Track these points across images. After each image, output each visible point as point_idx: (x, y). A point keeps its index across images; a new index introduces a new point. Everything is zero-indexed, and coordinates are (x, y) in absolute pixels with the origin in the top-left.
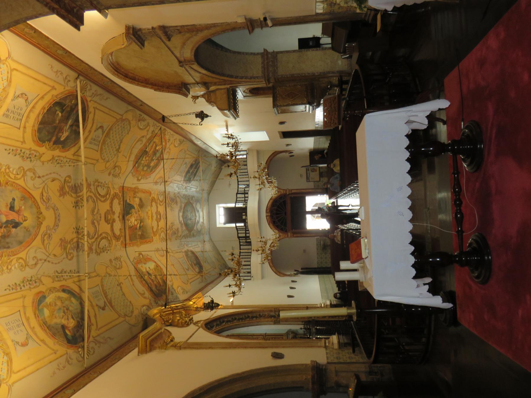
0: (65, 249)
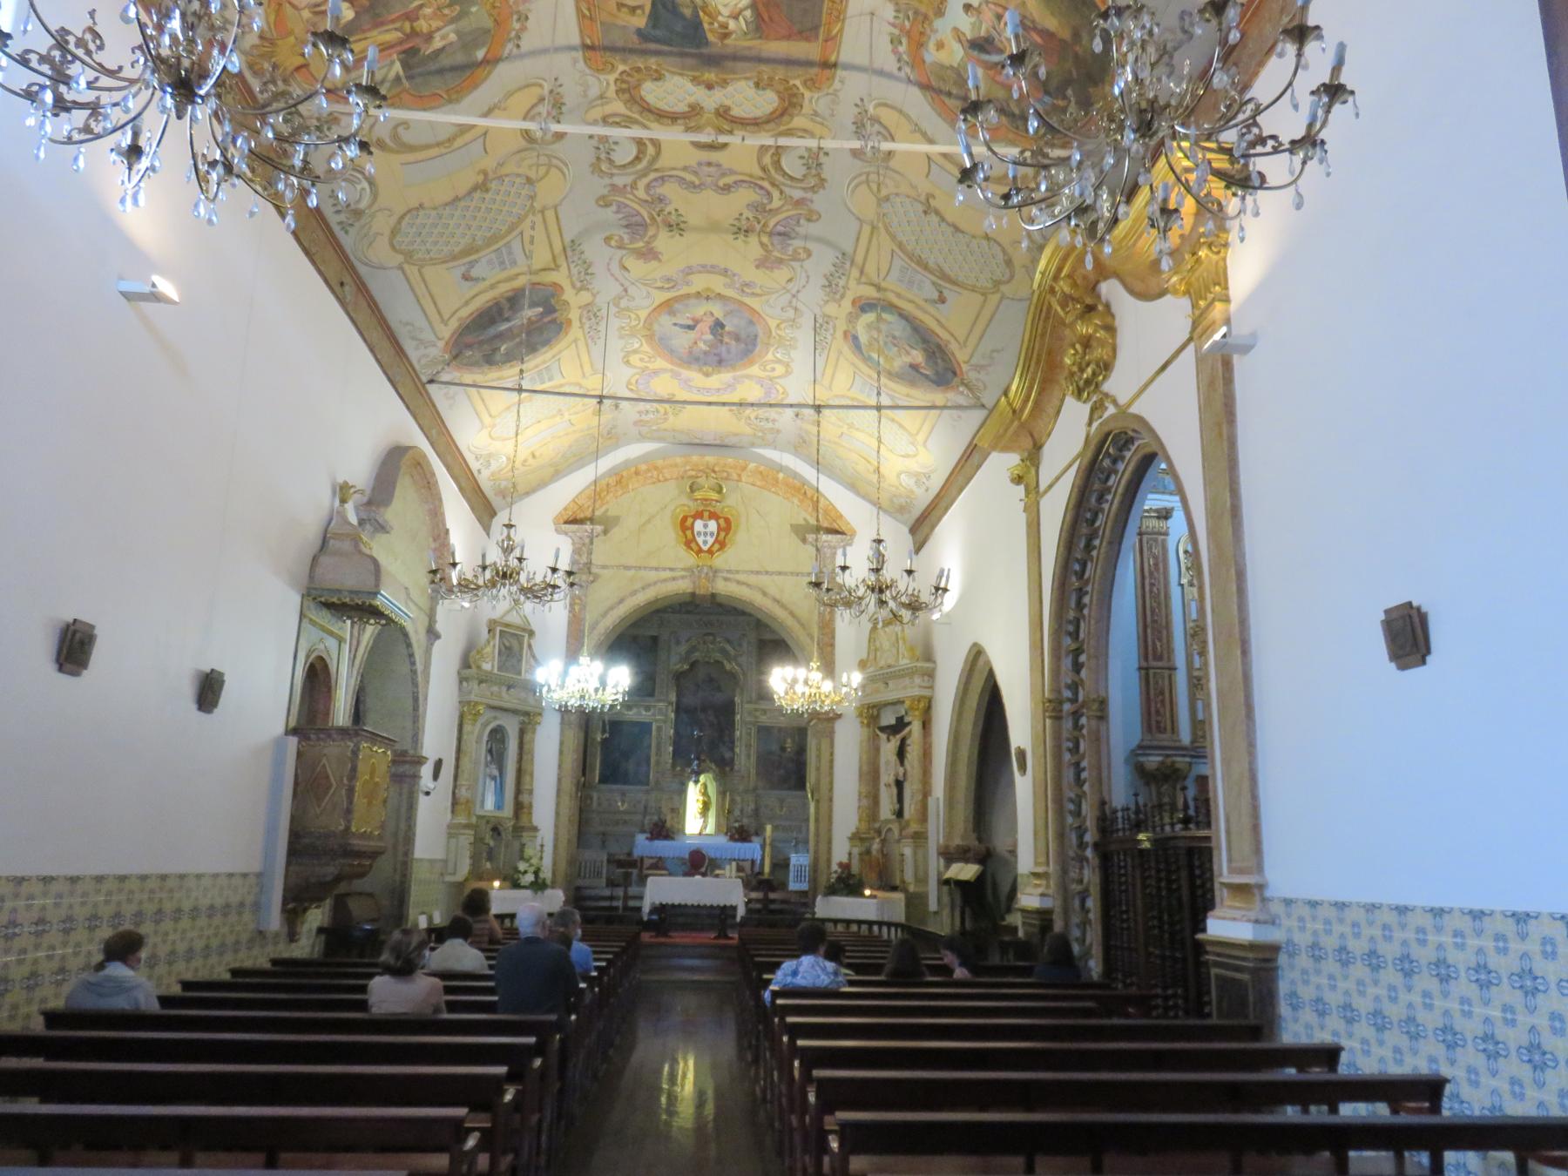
0: (781, 261)
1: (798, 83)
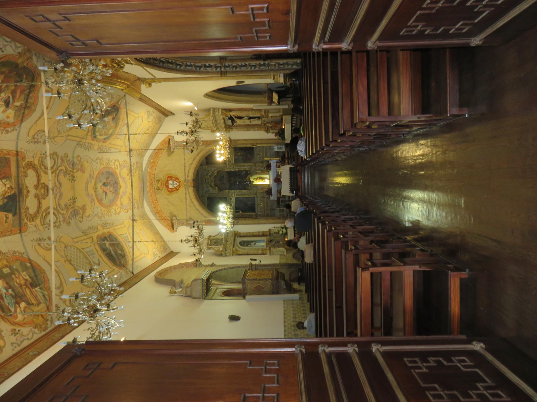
0: (82, 165)
1: (24, 163)
